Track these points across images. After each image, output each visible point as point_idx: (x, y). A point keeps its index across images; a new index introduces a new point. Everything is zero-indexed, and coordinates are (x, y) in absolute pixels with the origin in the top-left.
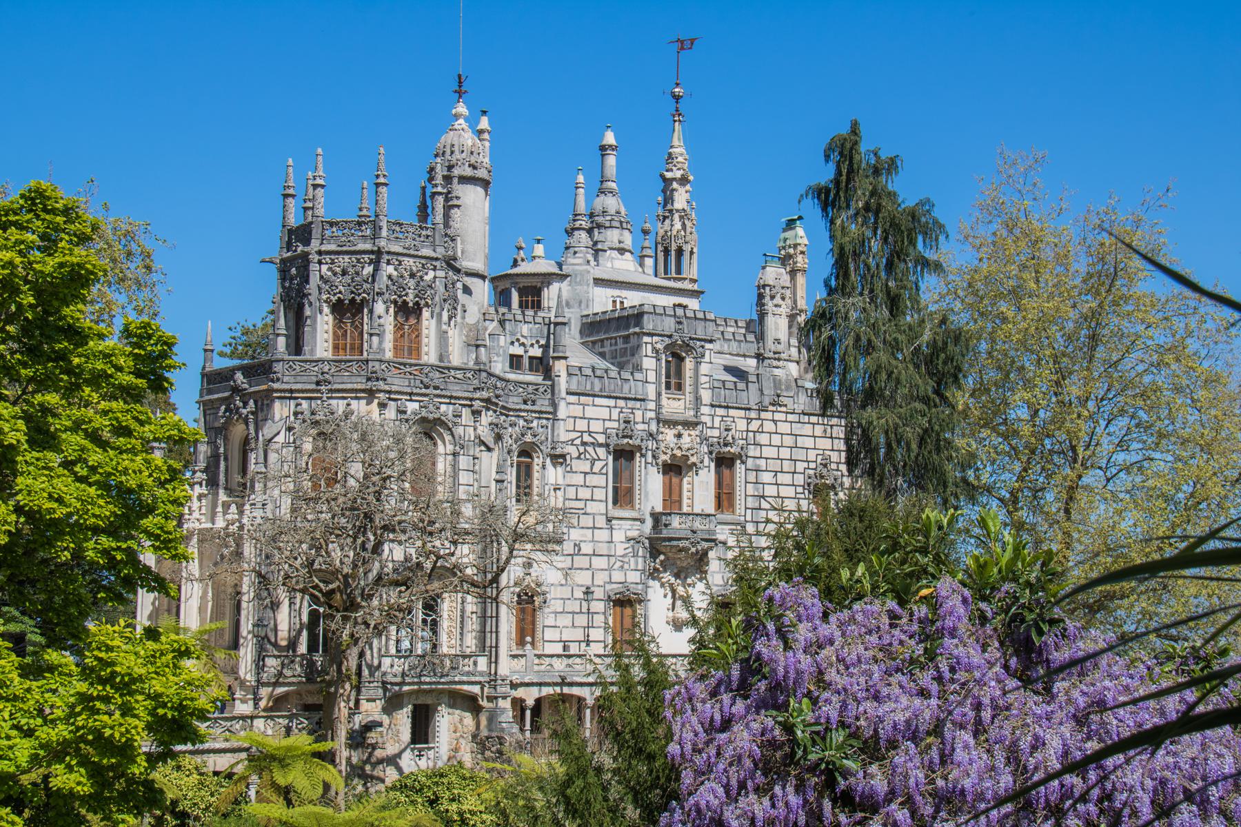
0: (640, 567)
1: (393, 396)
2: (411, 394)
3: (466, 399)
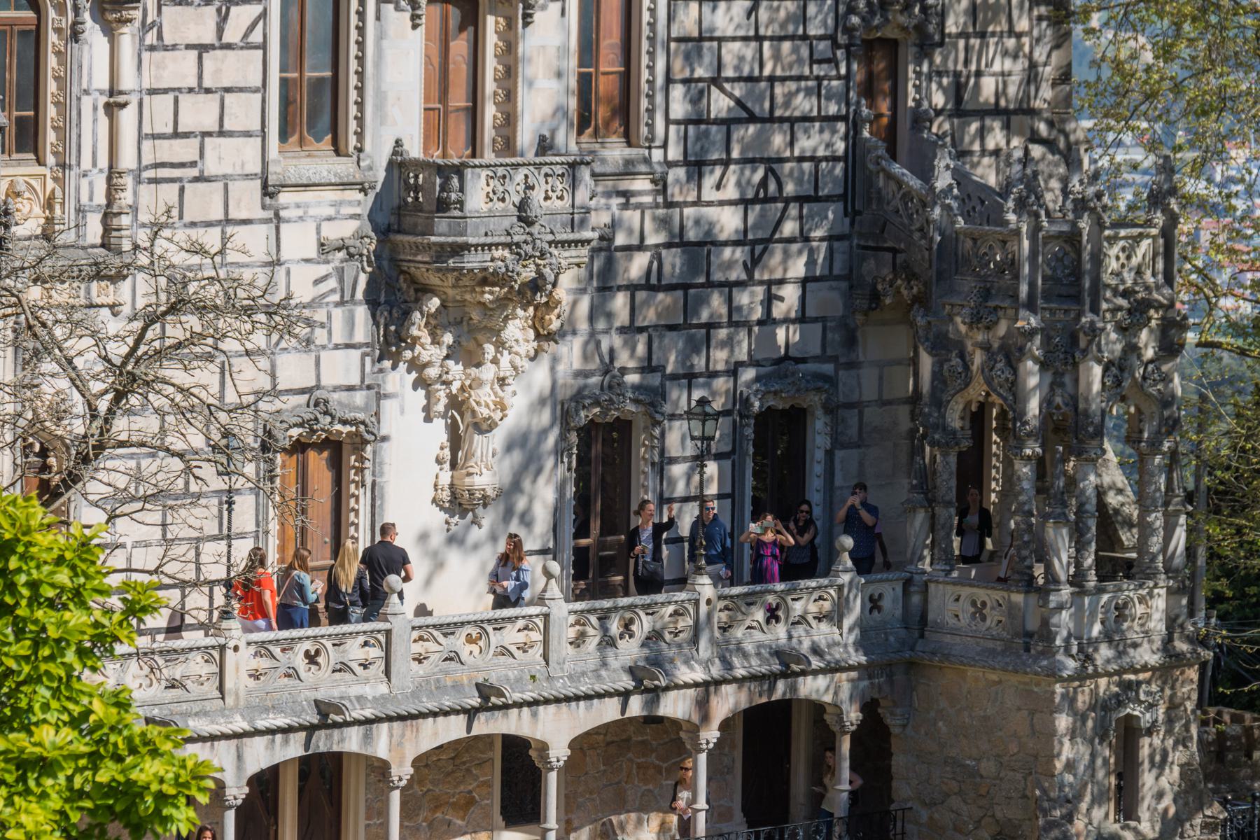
0: (361, 335)
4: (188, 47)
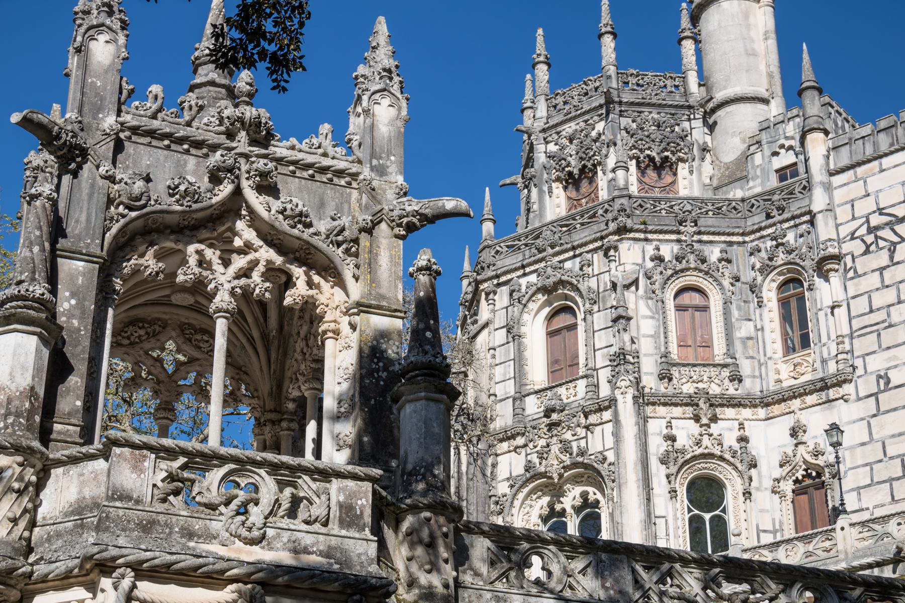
1: (503, 279)
2: (523, 267)
3: (595, 240)
4: (873, 271)
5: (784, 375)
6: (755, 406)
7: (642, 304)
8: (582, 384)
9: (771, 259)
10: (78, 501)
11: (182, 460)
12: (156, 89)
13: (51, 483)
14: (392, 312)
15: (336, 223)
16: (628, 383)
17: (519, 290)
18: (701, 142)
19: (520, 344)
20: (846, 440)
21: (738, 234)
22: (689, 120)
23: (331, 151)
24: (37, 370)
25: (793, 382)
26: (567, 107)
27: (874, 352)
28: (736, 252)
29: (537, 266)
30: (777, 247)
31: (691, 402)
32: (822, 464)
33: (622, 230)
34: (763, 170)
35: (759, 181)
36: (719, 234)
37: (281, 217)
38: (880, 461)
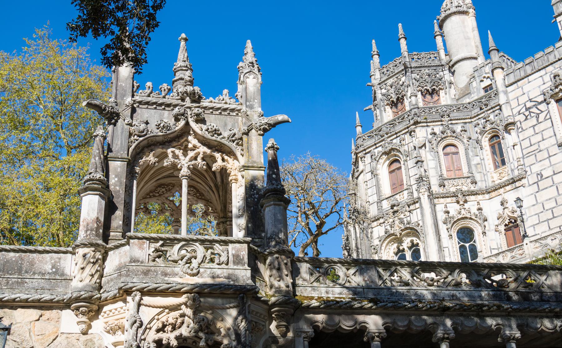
1: (367, 151)
2: (375, 144)
3: (405, 129)
5: (495, 179)
6: (484, 194)
7: (428, 154)
8: (406, 192)
9: (484, 128)
10: (119, 264)
11: (161, 242)
12: (149, 84)
13: (109, 258)
14: (259, 168)
15: (231, 132)
16: (425, 190)
17: (375, 155)
18: (449, 80)
19: (377, 178)
20: (525, 204)
21: (468, 118)
22: (443, 71)
23: (228, 101)
24: (99, 210)
25: (500, 181)
26: (388, 72)
27: (534, 164)
28: (468, 127)
29: (381, 143)
30: (486, 122)
31: (455, 195)
32: (516, 216)
33: (416, 123)
34: (477, 89)
35: (476, 94)
36: (460, 119)
37: (207, 132)
38: (542, 212)
